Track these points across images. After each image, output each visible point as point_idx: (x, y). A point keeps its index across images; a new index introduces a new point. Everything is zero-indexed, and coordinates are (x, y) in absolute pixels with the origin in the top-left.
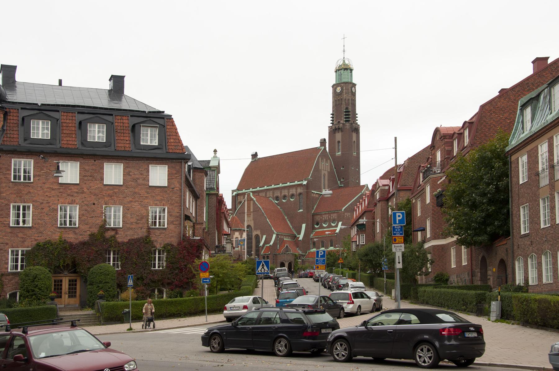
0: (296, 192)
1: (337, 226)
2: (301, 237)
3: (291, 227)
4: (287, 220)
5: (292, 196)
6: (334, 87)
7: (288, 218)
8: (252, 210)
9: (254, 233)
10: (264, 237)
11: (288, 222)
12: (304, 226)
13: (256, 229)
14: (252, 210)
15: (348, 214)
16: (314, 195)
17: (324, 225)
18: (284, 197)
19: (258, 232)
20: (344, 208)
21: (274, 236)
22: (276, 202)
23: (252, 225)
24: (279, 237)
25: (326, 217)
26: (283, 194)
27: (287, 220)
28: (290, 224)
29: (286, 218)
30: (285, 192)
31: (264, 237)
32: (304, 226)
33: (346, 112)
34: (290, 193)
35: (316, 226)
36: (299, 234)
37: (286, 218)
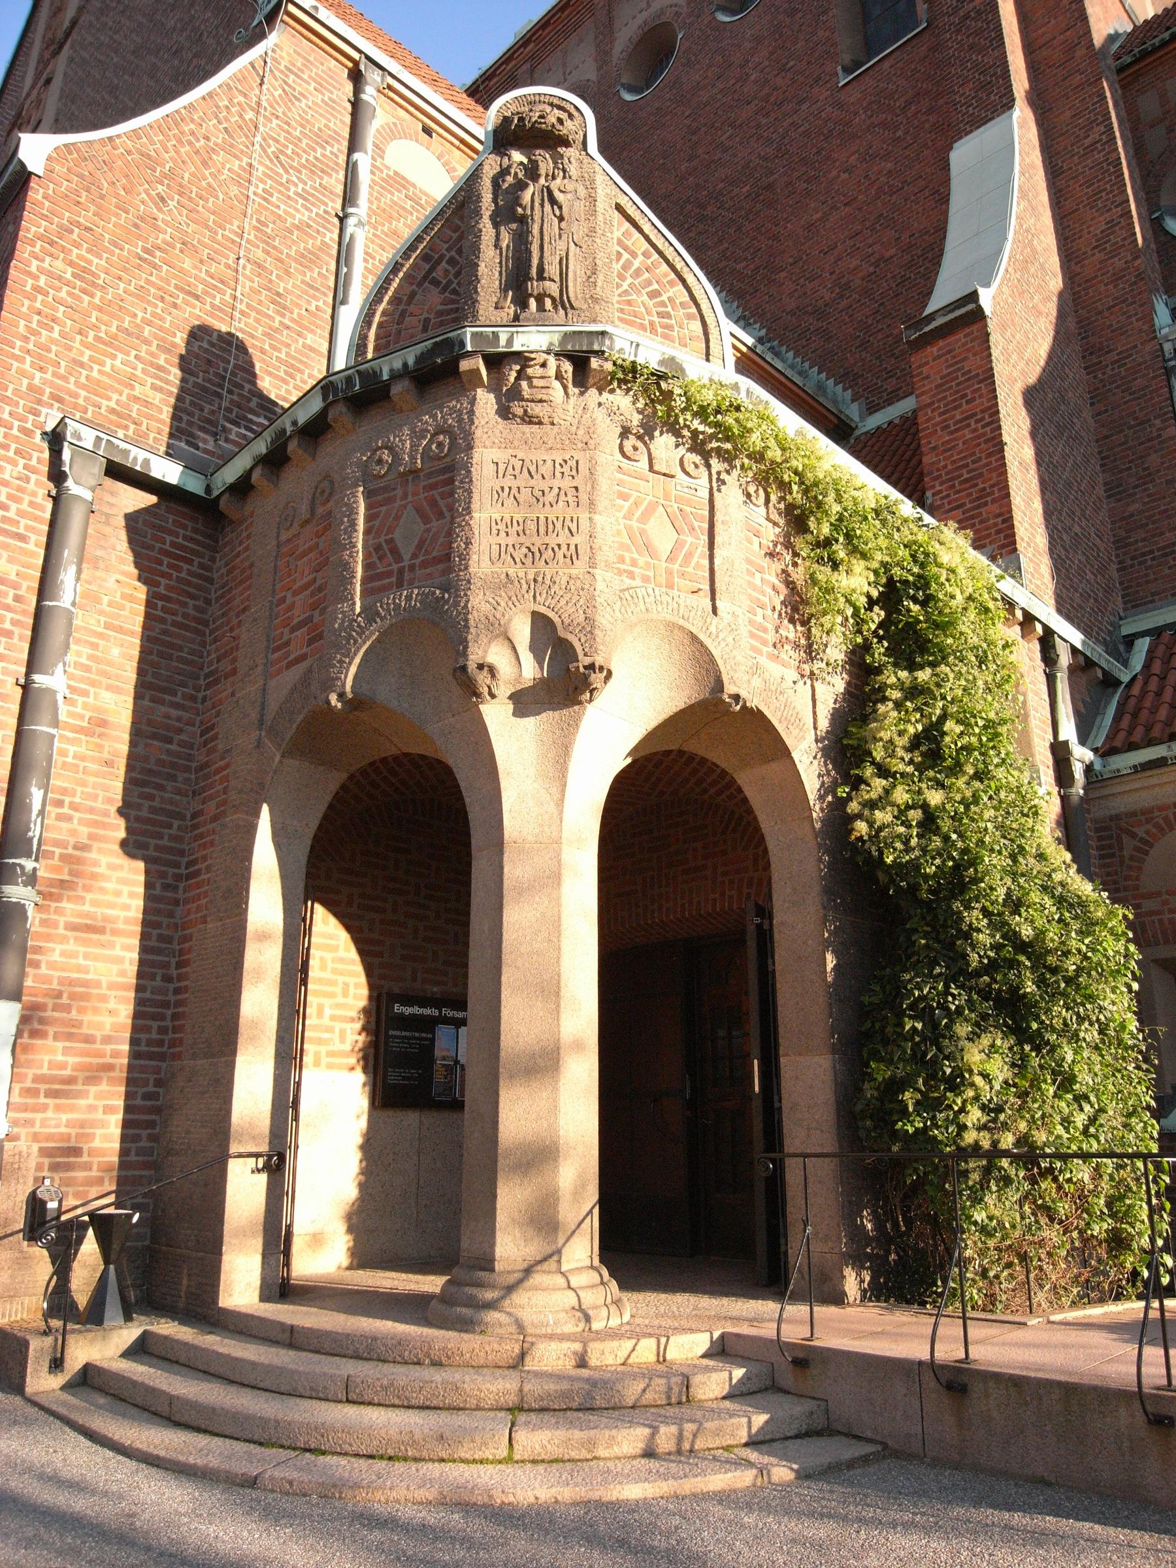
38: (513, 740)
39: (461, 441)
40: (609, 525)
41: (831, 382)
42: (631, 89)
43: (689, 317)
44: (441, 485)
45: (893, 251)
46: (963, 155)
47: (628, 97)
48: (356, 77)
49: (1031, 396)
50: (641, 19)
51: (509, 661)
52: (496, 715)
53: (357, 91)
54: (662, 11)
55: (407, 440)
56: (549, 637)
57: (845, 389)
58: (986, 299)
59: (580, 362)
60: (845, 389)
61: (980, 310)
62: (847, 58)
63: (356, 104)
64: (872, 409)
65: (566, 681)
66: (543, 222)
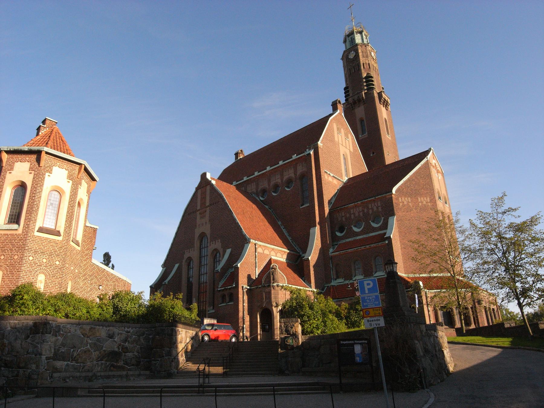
4: (282, 227)
5: (289, 182)
8: (208, 204)
10: (229, 251)
11: (284, 230)
14: (208, 204)
16: (330, 179)
17: (356, 229)
22: (262, 199)
23: (208, 232)
26: (272, 183)
27: (282, 227)
28: (286, 234)
29: (280, 223)
30: (277, 179)
31: (229, 251)
33: (366, 78)
34: (285, 178)
35: (338, 234)
37: (280, 223)
38: (274, 309)
39: (271, 291)
40: (280, 296)
42: (273, 192)
44: (270, 293)
46: (311, 230)
47: (274, 194)
48: (255, 244)
49: (314, 266)
50: (274, 182)
51: (274, 304)
52: (273, 308)
54: (277, 182)
55: (267, 290)
56: (276, 303)
58: (310, 258)
59: (278, 286)
65: (277, 306)
66: (275, 275)
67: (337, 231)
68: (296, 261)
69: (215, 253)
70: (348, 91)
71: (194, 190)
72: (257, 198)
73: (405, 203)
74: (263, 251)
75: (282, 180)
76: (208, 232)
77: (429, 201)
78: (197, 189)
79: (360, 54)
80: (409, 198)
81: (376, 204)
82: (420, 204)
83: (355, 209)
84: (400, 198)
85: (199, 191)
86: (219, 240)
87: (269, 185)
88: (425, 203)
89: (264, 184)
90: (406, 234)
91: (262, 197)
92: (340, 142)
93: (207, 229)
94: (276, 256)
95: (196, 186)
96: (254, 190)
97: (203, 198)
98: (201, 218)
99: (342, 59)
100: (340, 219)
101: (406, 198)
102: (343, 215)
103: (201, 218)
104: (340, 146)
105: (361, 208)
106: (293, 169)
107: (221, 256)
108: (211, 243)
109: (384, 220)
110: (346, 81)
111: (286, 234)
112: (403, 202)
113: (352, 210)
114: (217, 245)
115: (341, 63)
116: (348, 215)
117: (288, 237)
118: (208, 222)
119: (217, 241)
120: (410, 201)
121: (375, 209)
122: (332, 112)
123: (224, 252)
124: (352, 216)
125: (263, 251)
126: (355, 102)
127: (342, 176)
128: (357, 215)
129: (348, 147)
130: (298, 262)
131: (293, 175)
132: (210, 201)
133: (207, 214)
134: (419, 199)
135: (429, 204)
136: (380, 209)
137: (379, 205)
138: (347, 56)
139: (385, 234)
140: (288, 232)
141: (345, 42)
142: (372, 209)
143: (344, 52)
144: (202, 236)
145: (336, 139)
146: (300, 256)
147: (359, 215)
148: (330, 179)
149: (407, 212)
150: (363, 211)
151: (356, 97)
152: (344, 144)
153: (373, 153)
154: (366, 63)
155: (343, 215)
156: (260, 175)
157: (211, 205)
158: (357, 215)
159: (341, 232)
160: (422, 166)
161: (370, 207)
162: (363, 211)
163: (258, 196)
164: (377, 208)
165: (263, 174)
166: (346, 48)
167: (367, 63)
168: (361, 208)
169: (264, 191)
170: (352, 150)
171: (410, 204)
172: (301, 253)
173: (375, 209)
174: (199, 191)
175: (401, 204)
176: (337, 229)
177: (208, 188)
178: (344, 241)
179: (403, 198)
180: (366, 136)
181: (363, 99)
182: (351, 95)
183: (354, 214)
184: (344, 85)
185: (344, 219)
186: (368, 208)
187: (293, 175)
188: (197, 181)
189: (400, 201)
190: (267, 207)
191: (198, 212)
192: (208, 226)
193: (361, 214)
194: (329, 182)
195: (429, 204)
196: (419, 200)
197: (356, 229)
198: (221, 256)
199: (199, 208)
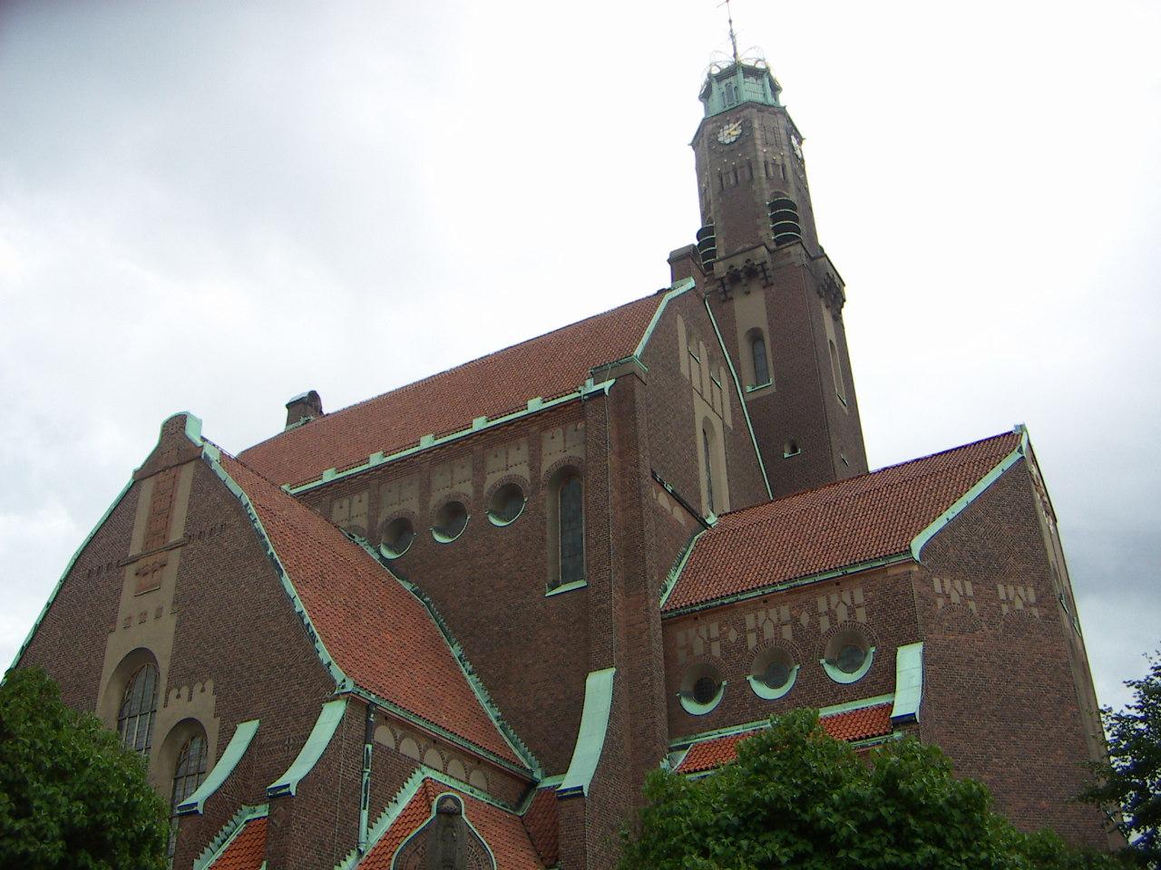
0: (534, 463)
1: (885, 680)
2: (581, 772)
3: (492, 714)
5: (509, 495)
6: (705, 141)
7: (468, 655)
9: (173, 710)
10: (245, 733)
11: (472, 681)
12: (600, 686)
13: (184, 676)
14: (176, 534)
15: (953, 589)
17: (763, 691)
18: (453, 512)
19: (201, 703)
20: (917, 544)
21: (332, 715)
23: (163, 652)
24: (383, 735)
25: (770, 624)
27: (465, 668)
28: (481, 697)
29: (456, 651)
30: (458, 483)
31: (245, 733)
32: (600, 686)
33: (773, 206)
35: (692, 707)
36: (560, 761)
41: (529, 754)
42: (442, 532)
43: (487, 864)
45: (561, 697)
53: (368, 716)
54: (459, 495)
57: (536, 760)
60: (536, 760)
61: (583, 794)
62: (550, 579)
63: (367, 721)
64: (547, 775)
67: (688, 696)
68: (519, 806)
69: (183, 738)
70: (712, 242)
71: (125, 480)
72: (370, 551)
73: (955, 598)
74: (398, 742)
75: (478, 488)
76: (163, 652)
77: (1032, 599)
78: (140, 476)
79: (758, 134)
80: (968, 584)
81: (846, 597)
82: (1005, 608)
83: (762, 615)
84: (936, 581)
85: (148, 486)
86: (210, 685)
87: (424, 503)
88: (1019, 605)
89: (404, 500)
90: (960, 713)
91: (390, 547)
92: (696, 384)
93: (160, 637)
94: (445, 772)
95: (138, 465)
96: (363, 522)
97: (161, 515)
98: (142, 592)
99: (695, 144)
100: (699, 649)
101: (958, 583)
102: (715, 633)
103: (142, 592)
104: (697, 398)
105: (785, 612)
106: (524, 448)
107: (212, 750)
108: (174, 692)
109: (877, 659)
110: (704, 215)
111: (478, 695)
112: (949, 597)
113: (750, 621)
114: (201, 703)
115: (690, 157)
116: (733, 636)
117: (487, 707)
118: (167, 609)
119: (198, 687)
120: (970, 592)
121: (842, 614)
122: (668, 285)
123: (227, 736)
124: (752, 640)
125: (398, 742)
126: (734, 277)
127: (699, 501)
128: (769, 633)
129: (718, 409)
130: (528, 804)
131: (523, 472)
132: (190, 521)
133: (169, 578)
134: (1000, 587)
135: (1035, 612)
136: (861, 616)
137: (859, 597)
138: (715, 134)
139: (890, 706)
140: (490, 687)
141: (706, 95)
142: (831, 614)
143: (704, 123)
144: (139, 660)
145: (684, 370)
146: (534, 783)
147: (778, 635)
148: (663, 500)
149: (962, 632)
150: (795, 621)
151: (739, 262)
152: (707, 396)
153: (794, 449)
154: (774, 164)
155: (715, 633)
156: (391, 464)
157: (189, 537)
158: (769, 633)
159: (703, 698)
160: (1006, 473)
161: (822, 605)
162: (795, 621)
163: (374, 544)
164: (852, 611)
165: (403, 460)
166: (707, 109)
167: (779, 163)
168: (785, 612)
169: (400, 530)
170: (729, 422)
171: (972, 605)
172: (537, 775)
173: (842, 614)
174: (148, 486)
175: (940, 602)
176: (686, 685)
177: (187, 474)
178: (715, 735)
179: (947, 583)
180: (772, 390)
181: (764, 271)
182: (721, 254)
183: (759, 631)
184: (698, 226)
185: (716, 649)
186: (815, 613)
187: (523, 472)
188: (143, 444)
189: (938, 589)
190: (408, 586)
191: (131, 569)
192: (169, 623)
193: (787, 632)
194: (658, 511)
195: (1035, 612)
196: (1002, 596)
197: (763, 691)
198: (212, 750)
199: (135, 550)
